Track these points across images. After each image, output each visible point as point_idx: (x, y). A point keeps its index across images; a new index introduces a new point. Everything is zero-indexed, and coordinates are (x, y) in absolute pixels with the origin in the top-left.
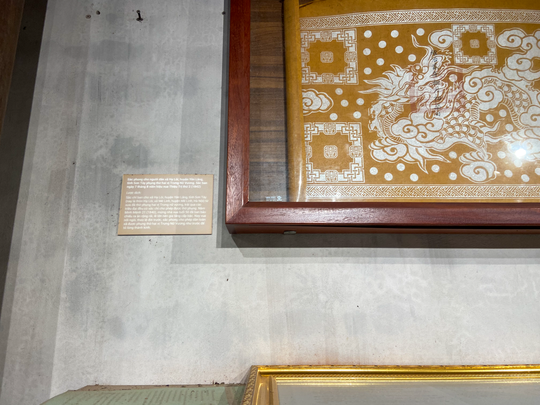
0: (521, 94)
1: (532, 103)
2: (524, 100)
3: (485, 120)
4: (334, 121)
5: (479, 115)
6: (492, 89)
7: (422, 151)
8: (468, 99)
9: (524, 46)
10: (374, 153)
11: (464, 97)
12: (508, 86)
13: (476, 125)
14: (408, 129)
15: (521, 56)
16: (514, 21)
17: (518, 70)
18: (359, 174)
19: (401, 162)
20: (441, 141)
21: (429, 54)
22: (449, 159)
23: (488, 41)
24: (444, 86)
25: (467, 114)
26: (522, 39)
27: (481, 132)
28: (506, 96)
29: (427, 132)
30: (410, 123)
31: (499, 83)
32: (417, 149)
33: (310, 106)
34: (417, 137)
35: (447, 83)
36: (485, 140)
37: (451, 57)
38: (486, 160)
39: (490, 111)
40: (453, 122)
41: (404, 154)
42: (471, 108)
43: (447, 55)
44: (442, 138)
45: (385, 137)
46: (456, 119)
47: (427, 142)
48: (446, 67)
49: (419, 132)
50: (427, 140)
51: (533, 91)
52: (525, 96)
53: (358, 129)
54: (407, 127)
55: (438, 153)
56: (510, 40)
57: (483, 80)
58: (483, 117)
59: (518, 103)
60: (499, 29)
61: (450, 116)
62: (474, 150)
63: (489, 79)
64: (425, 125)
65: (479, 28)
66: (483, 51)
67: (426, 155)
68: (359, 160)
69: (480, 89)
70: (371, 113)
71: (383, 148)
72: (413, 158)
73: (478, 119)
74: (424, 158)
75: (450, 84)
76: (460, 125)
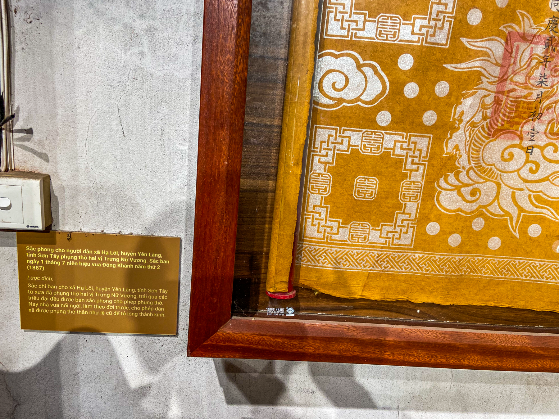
4: (383, 128)
10: (442, 198)
18: (407, 232)
19: (481, 215)
30: (517, 141)
32: (513, 193)
33: (342, 89)
34: (521, 172)
47: (531, 182)
49: (527, 161)
53: (425, 149)
54: (507, 151)
55: (551, 204)
67: (527, 206)
68: (412, 207)
72: (503, 210)
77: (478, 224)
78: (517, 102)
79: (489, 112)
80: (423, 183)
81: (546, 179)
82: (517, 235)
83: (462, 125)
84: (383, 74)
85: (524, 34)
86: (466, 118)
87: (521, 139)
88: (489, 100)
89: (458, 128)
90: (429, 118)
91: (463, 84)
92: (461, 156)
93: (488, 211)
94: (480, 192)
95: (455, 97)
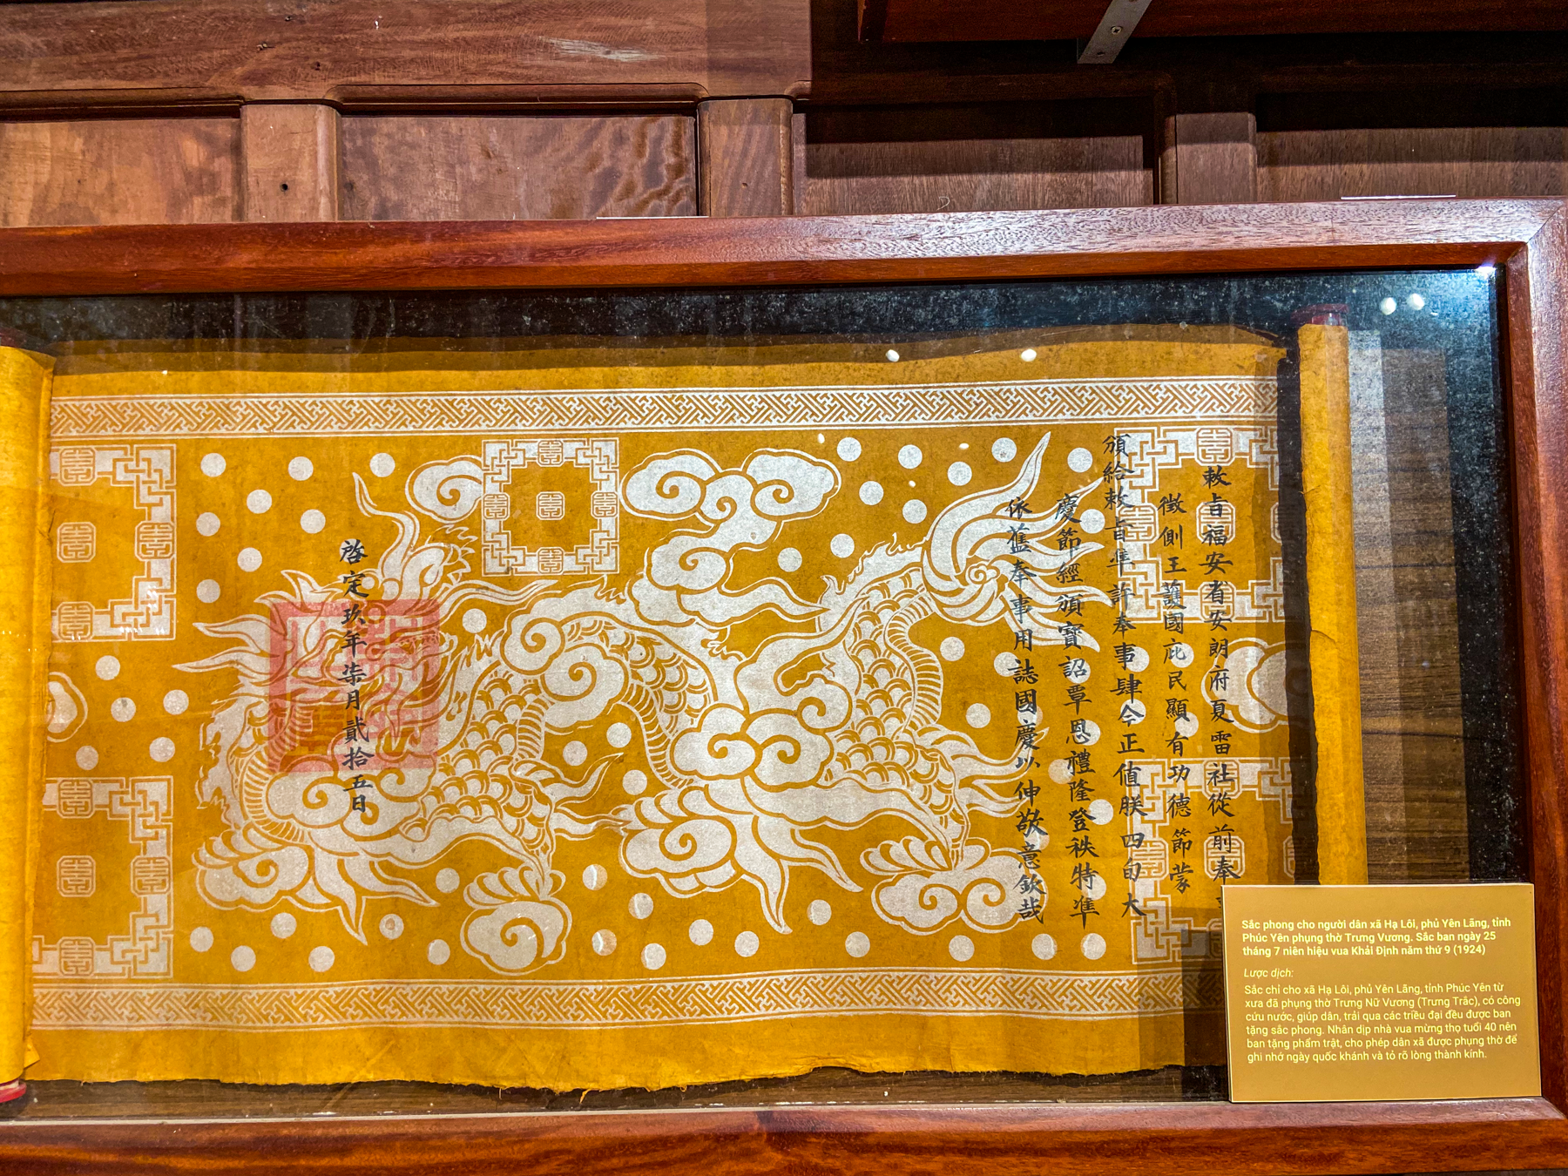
1: (716, 699)
2: (693, 689)
5: (542, 743)
6: (595, 657)
7: (359, 867)
8: (515, 692)
9: (709, 508)
11: (504, 685)
12: (646, 642)
13: (531, 777)
17: (681, 590)
20: (418, 833)
21: (406, 541)
22: (435, 893)
23: (595, 495)
24: (444, 647)
25: (507, 742)
26: (703, 484)
27: (544, 799)
31: (618, 636)
32: (341, 864)
35: (455, 639)
36: (553, 826)
37: (471, 551)
38: (542, 897)
40: (465, 766)
41: (297, 882)
42: (522, 722)
43: (460, 544)
44: (422, 824)
45: (243, 823)
46: (473, 756)
48: (456, 584)
51: (725, 658)
54: (315, 790)
55: (407, 874)
56: (666, 491)
59: (670, 698)
60: (635, 452)
61: (458, 748)
62: (513, 862)
63: (586, 622)
69: (555, 655)
70: (210, 739)
71: (234, 863)
72: (327, 895)
73: (538, 758)
74: (360, 891)
75: (466, 639)
76: (482, 777)
77: (284, 925)
78: (311, 708)
79: (264, 730)
80: (170, 859)
83: (223, 753)
84: (77, 691)
85: (303, 604)
86: (225, 742)
88: (262, 711)
89: (216, 761)
92: (228, 807)
93: (296, 898)
94: (275, 866)
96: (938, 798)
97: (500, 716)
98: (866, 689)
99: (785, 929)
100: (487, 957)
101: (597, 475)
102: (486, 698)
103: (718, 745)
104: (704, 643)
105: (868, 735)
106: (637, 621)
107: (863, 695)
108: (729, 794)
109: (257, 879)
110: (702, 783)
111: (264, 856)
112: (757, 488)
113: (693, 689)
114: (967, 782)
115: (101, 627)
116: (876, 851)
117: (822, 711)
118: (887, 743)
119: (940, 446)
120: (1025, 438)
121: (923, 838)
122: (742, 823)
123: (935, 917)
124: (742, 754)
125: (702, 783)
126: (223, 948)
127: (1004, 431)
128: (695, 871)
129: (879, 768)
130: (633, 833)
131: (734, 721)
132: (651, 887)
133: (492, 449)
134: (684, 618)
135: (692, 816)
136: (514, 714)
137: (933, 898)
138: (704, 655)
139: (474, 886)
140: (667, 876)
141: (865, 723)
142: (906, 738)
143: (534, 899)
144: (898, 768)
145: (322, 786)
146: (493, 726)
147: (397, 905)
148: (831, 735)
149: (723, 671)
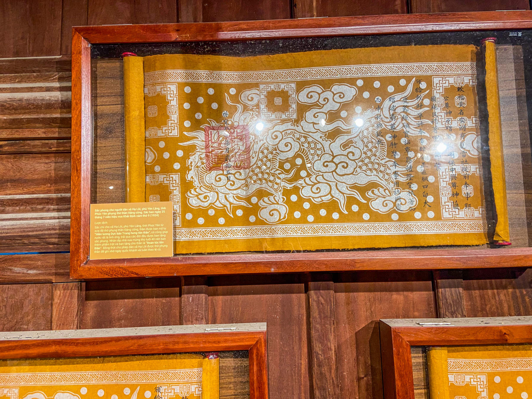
0: (315, 144)
2: (318, 149)
3: (283, 168)
4: (157, 173)
9: (321, 101)
14: (220, 178)
15: (319, 110)
16: (314, 78)
17: (314, 123)
19: (212, 207)
21: (240, 111)
22: (251, 203)
23: (290, 98)
25: (268, 164)
26: (319, 94)
27: (279, 178)
28: (303, 146)
29: (235, 180)
32: (225, 196)
34: (227, 186)
36: (282, 185)
39: (287, 160)
43: (253, 111)
45: (199, 186)
50: (233, 188)
51: (327, 141)
52: (319, 146)
54: (217, 178)
57: (283, 133)
58: (281, 166)
60: (301, 86)
61: (255, 166)
62: (272, 195)
63: (289, 132)
64: (234, 174)
65: (282, 86)
66: (285, 107)
71: (197, 196)
77: (211, 212)
78: (216, 155)
81: (239, 188)
82: (231, 215)
87: (223, 170)
88: (203, 156)
90: (177, 166)
91: (190, 150)
95: (186, 156)
96: (387, 177)
97: (267, 157)
98: (365, 149)
99: (346, 212)
100: (266, 220)
101: (290, 93)
102: (262, 152)
103: (325, 164)
104: (321, 137)
105: (367, 161)
106: (302, 132)
107: (365, 150)
108: (328, 176)
109: (204, 200)
110: (321, 174)
111: (206, 194)
112: (334, 95)
113: (318, 149)
114: (395, 173)
115: (160, 134)
116: (370, 192)
117: (354, 155)
118: (372, 163)
119: (386, 81)
120: (408, 79)
121: (383, 188)
122: (333, 185)
123: (386, 209)
124: (332, 166)
125: (321, 174)
126: (195, 218)
127: (403, 77)
128: (320, 197)
129: (370, 170)
130: (303, 187)
131: (329, 158)
132: (309, 200)
133: (261, 87)
134: (316, 131)
135: (319, 182)
136: (270, 156)
137: (386, 204)
138: (320, 140)
139: (261, 201)
140: (313, 198)
141: (366, 158)
142: (378, 161)
143: (278, 204)
144: (376, 170)
145: (221, 176)
146: (265, 159)
147: (240, 207)
148: (356, 161)
149: (326, 144)
